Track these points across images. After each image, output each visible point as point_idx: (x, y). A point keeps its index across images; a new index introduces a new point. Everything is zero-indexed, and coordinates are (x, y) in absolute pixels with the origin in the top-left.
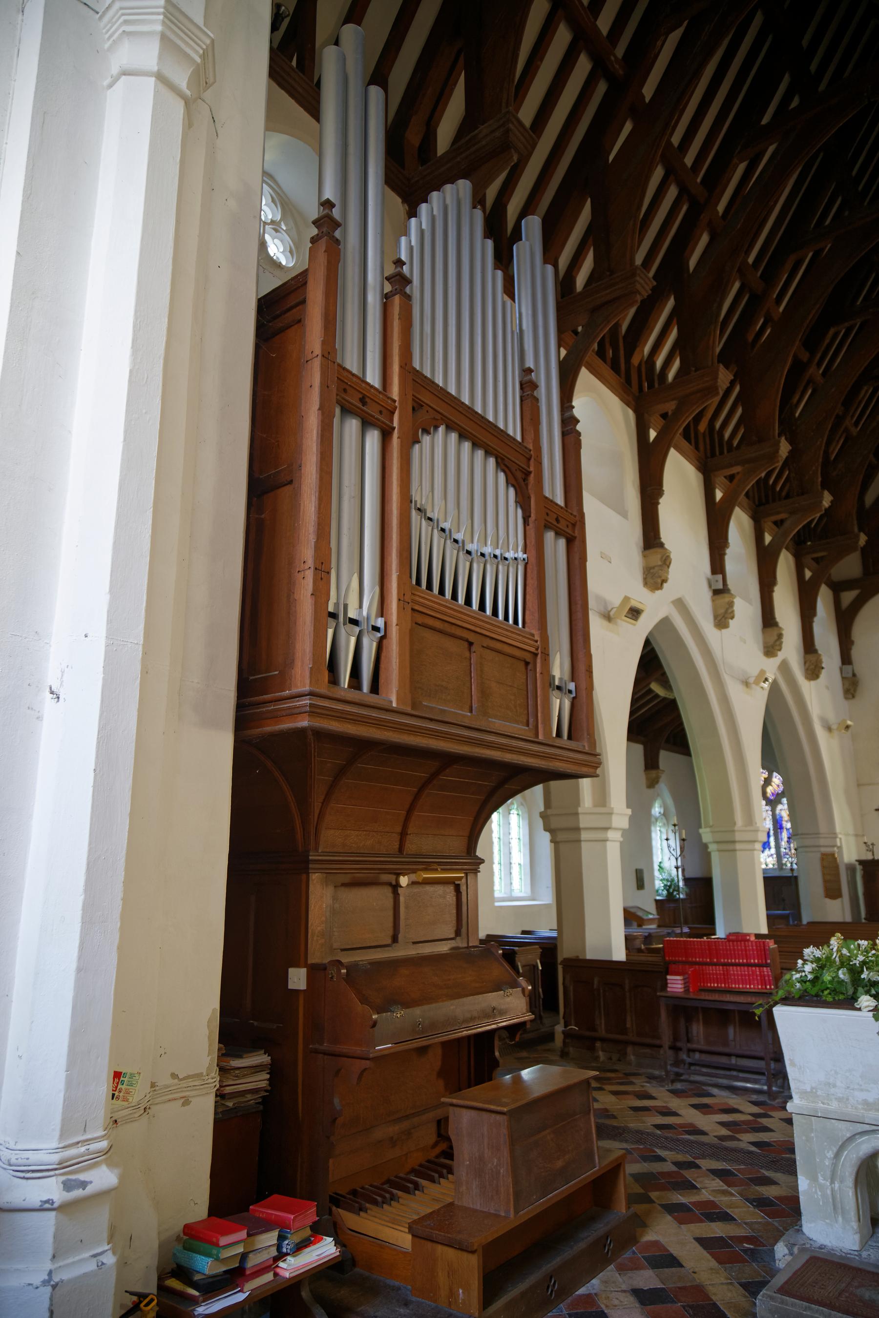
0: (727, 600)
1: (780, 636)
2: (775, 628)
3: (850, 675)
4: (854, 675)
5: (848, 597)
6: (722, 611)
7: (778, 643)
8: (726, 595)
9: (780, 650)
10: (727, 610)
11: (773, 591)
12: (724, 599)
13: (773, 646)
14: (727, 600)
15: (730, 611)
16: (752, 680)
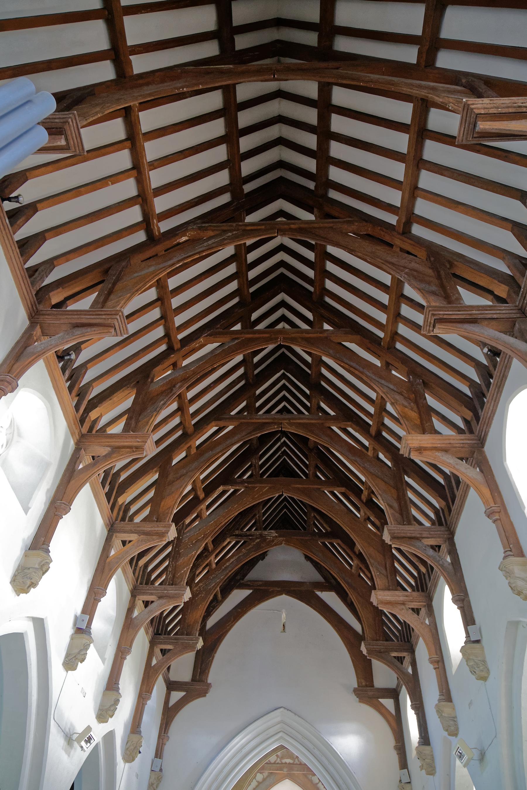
0: (84, 641)
1: (117, 702)
2: (115, 693)
3: (158, 769)
4: (161, 770)
5: (177, 696)
6: (76, 651)
7: (112, 708)
8: (85, 636)
9: (111, 716)
10: (81, 650)
11: (125, 658)
12: (82, 639)
13: (107, 710)
14: (84, 641)
15: (83, 653)
16: (75, 736)
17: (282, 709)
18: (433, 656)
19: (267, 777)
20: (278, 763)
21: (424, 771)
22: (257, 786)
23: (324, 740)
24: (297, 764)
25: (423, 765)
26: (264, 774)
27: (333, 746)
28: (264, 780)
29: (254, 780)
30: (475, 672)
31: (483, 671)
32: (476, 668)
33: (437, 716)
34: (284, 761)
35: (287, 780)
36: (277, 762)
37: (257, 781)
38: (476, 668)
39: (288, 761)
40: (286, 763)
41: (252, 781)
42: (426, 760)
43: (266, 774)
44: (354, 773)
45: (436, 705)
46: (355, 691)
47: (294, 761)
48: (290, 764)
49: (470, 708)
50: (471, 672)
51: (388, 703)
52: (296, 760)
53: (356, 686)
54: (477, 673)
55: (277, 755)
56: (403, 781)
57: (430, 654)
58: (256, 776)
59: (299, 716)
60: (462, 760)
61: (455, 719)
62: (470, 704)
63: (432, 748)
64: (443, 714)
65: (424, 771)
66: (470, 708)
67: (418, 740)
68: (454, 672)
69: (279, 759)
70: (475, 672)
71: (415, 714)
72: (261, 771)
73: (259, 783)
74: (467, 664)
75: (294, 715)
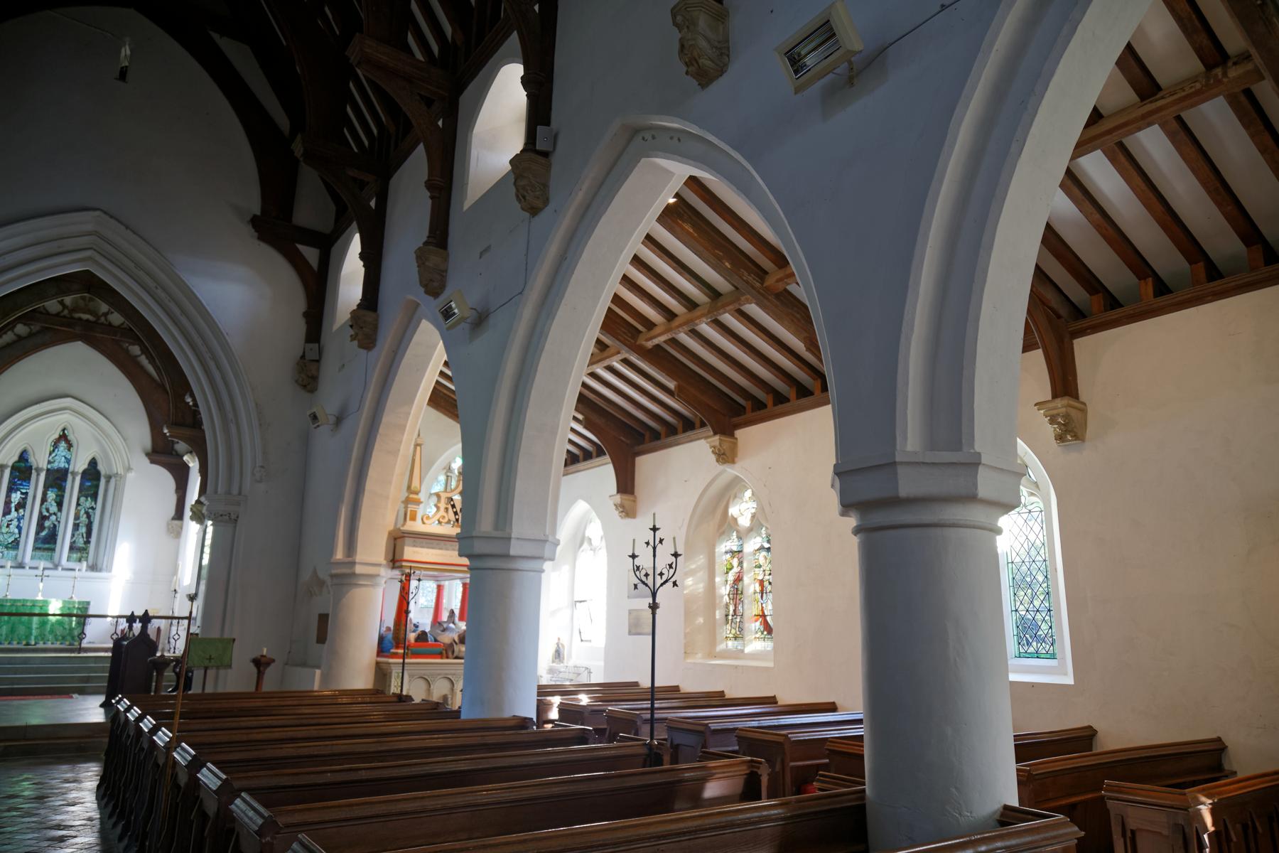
17: (97, 213)
18: (437, 179)
19: (38, 332)
20: (64, 317)
21: (356, 343)
22: (14, 342)
23: (181, 279)
24: (102, 324)
25: (357, 334)
26: (32, 327)
27: (195, 292)
28: (31, 335)
29: (10, 333)
30: (524, 197)
31: (538, 198)
32: (529, 192)
33: (416, 264)
34: (77, 315)
35: (80, 342)
36: (62, 314)
37: (15, 334)
38: (529, 192)
39: (85, 316)
40: (80, 319)
41: (5, 333)
42: (364, 329)
43: (36, 327)
44: (225, 335)
45: (420, 248)
46: (255, 222)
47: (98, 318)
48: (88, 321)
49: (480, 257)
50: (517, 196)
51: (311, 254)
52: (103, 319)
53: (258, 213)
54: (527, 198)
55: (62, 303)
56: (308, 357)
57: (430, 173)
58: (15, 326)
59: (134, 233)
60: (446, 320)
61: (444, 274)
62: (487, 249)
63: (378, 316)
64: (427, 263)
65: (356, 343)
66: (480, 257)
67: (359, 301)
68: (466, 207)
69: (66, 312)
70: (524, 197)
71: (364, 266)
72: (24, 319)
73: (20, 338)
74: (515, 183)
75: (123, 228)
